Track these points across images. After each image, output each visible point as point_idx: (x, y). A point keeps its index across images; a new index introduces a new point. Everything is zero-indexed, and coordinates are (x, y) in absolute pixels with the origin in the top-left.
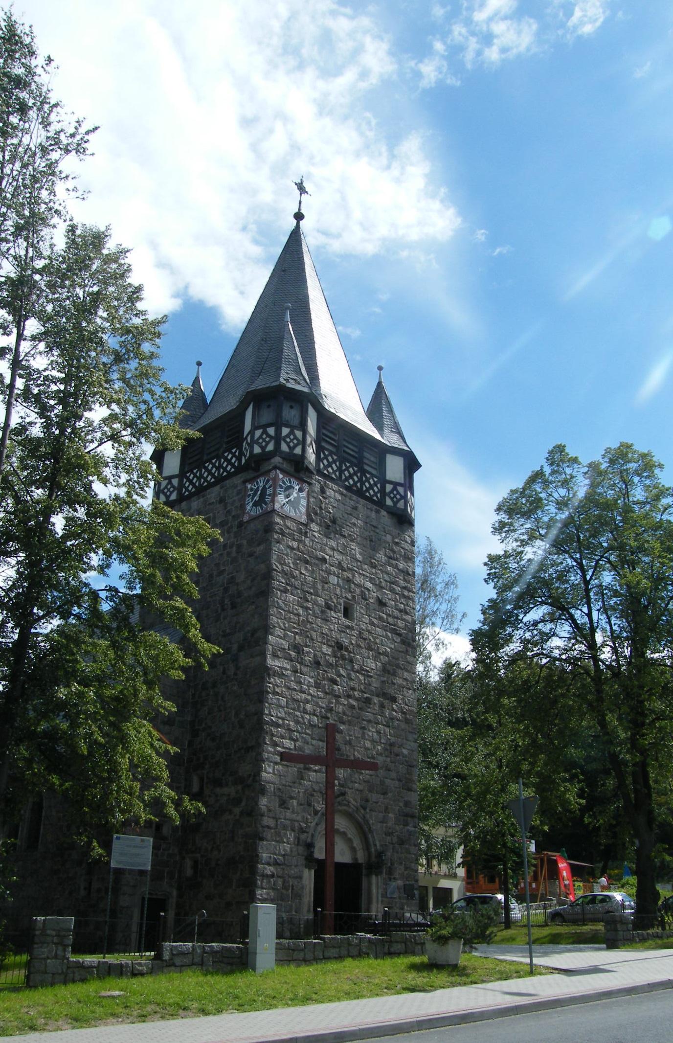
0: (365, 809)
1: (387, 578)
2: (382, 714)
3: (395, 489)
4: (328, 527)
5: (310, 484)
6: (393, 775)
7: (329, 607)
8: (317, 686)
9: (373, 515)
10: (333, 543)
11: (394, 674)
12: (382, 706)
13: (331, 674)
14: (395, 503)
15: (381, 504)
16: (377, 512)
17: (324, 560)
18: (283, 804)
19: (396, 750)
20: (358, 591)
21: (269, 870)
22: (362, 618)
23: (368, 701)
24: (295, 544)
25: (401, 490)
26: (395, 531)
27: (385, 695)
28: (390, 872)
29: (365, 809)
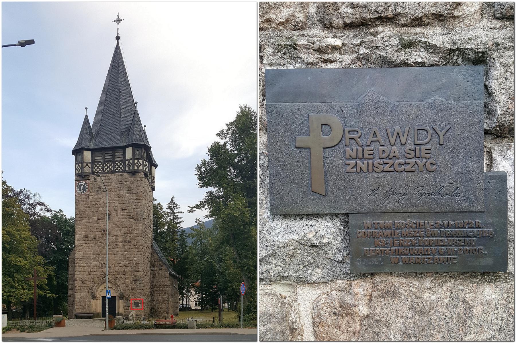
0: (116, 280)
1: (126, 199)
2: (124, 248)
3: (129, 162)
4: (98, 191)
5: (89, 180)
6: (129, 267)
7: (99, 219)
8: (95, 245)
9: (120, 177)
10: (100, 196)
11: (131, 233)
12: (124, 246)
13: (102, 240)
14: (129, 168)
15: (124, 171)
16: (122, 175)
17: (96, 204)
18: (83, 282)
19: (131, 259)
20: (112, 209)
21: (78, 300)
22: (115, 218)
23: (117, 245)
24: (84, 203)
25: (131, 161)
26: (131, 179)
27: (125, 242)
28: (127, 298)
29: (116, 280)
